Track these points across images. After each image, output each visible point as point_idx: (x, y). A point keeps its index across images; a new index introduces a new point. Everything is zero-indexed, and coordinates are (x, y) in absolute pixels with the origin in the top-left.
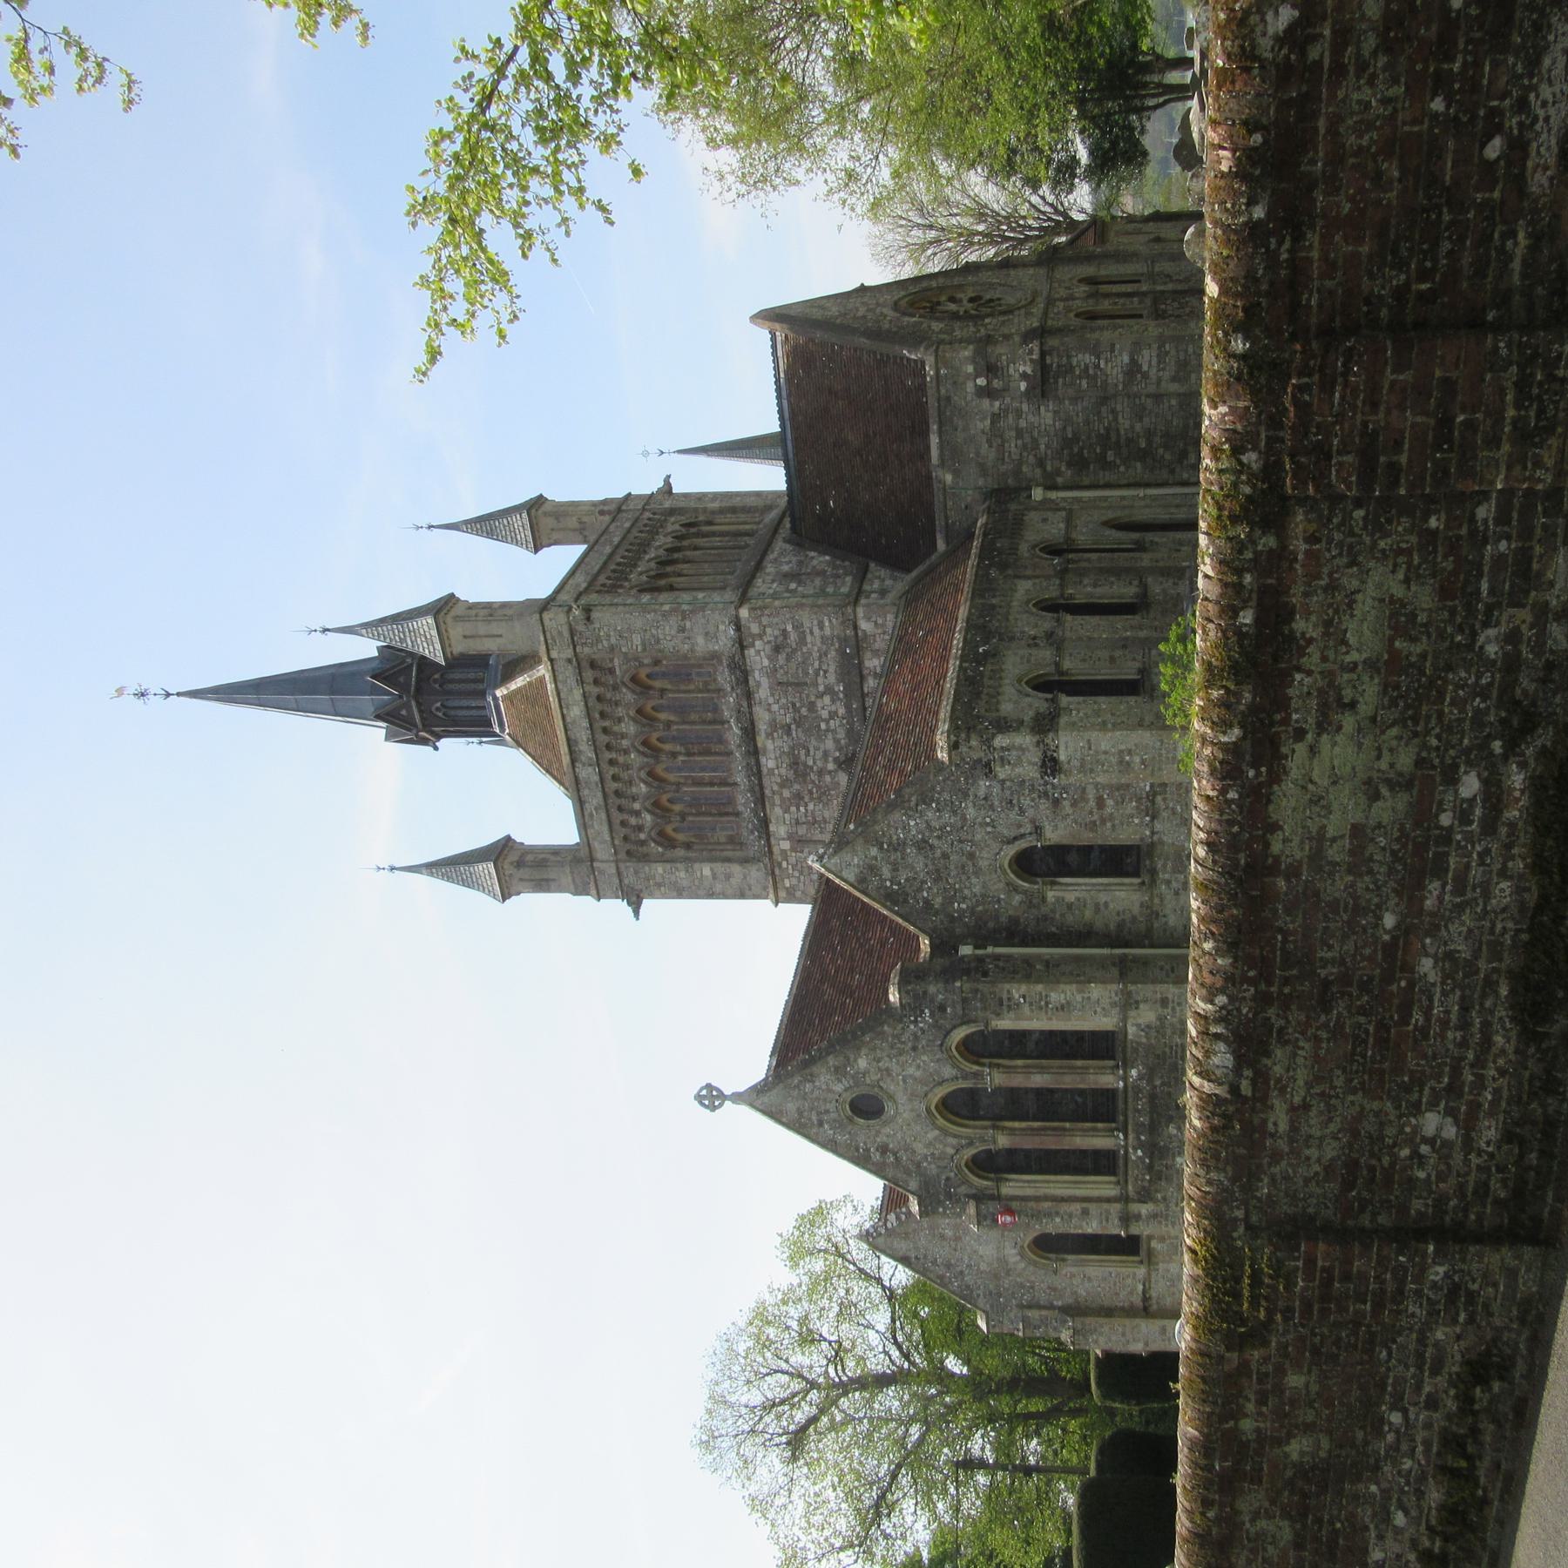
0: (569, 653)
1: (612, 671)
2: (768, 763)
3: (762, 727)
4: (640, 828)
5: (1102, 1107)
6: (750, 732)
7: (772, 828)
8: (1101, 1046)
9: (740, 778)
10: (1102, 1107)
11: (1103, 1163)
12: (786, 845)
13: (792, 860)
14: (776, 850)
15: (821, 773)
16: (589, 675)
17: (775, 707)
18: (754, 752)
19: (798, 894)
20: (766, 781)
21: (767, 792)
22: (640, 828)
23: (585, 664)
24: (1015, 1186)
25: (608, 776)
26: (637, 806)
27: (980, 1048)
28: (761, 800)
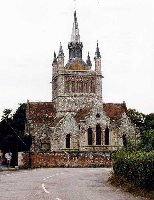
0: (96, 74)
1: (93, 79)
2: (81, 98)
3: (86, 98)
4: (69, 79)
5: (99, 143)
6: (85, 96)
7: (71, 97)
8: (107, 143)
9: (78, 94)
10: (99, 143)
11: (90, 143)
12: (68, 99)
13: (65, 99)
14: (67, 97)
15: (79, 105)
16: (93, 76)
17: (89, 100)
18: (82, 97)
19: (60, 100)
20: (78, 98)
21: (76, 97)
22: (69, 79)
23: (95, 76)
24: (86, 133)
25: (78, 76)
26: (73, 79)
27: (107, 131)
28: (75, 96)
